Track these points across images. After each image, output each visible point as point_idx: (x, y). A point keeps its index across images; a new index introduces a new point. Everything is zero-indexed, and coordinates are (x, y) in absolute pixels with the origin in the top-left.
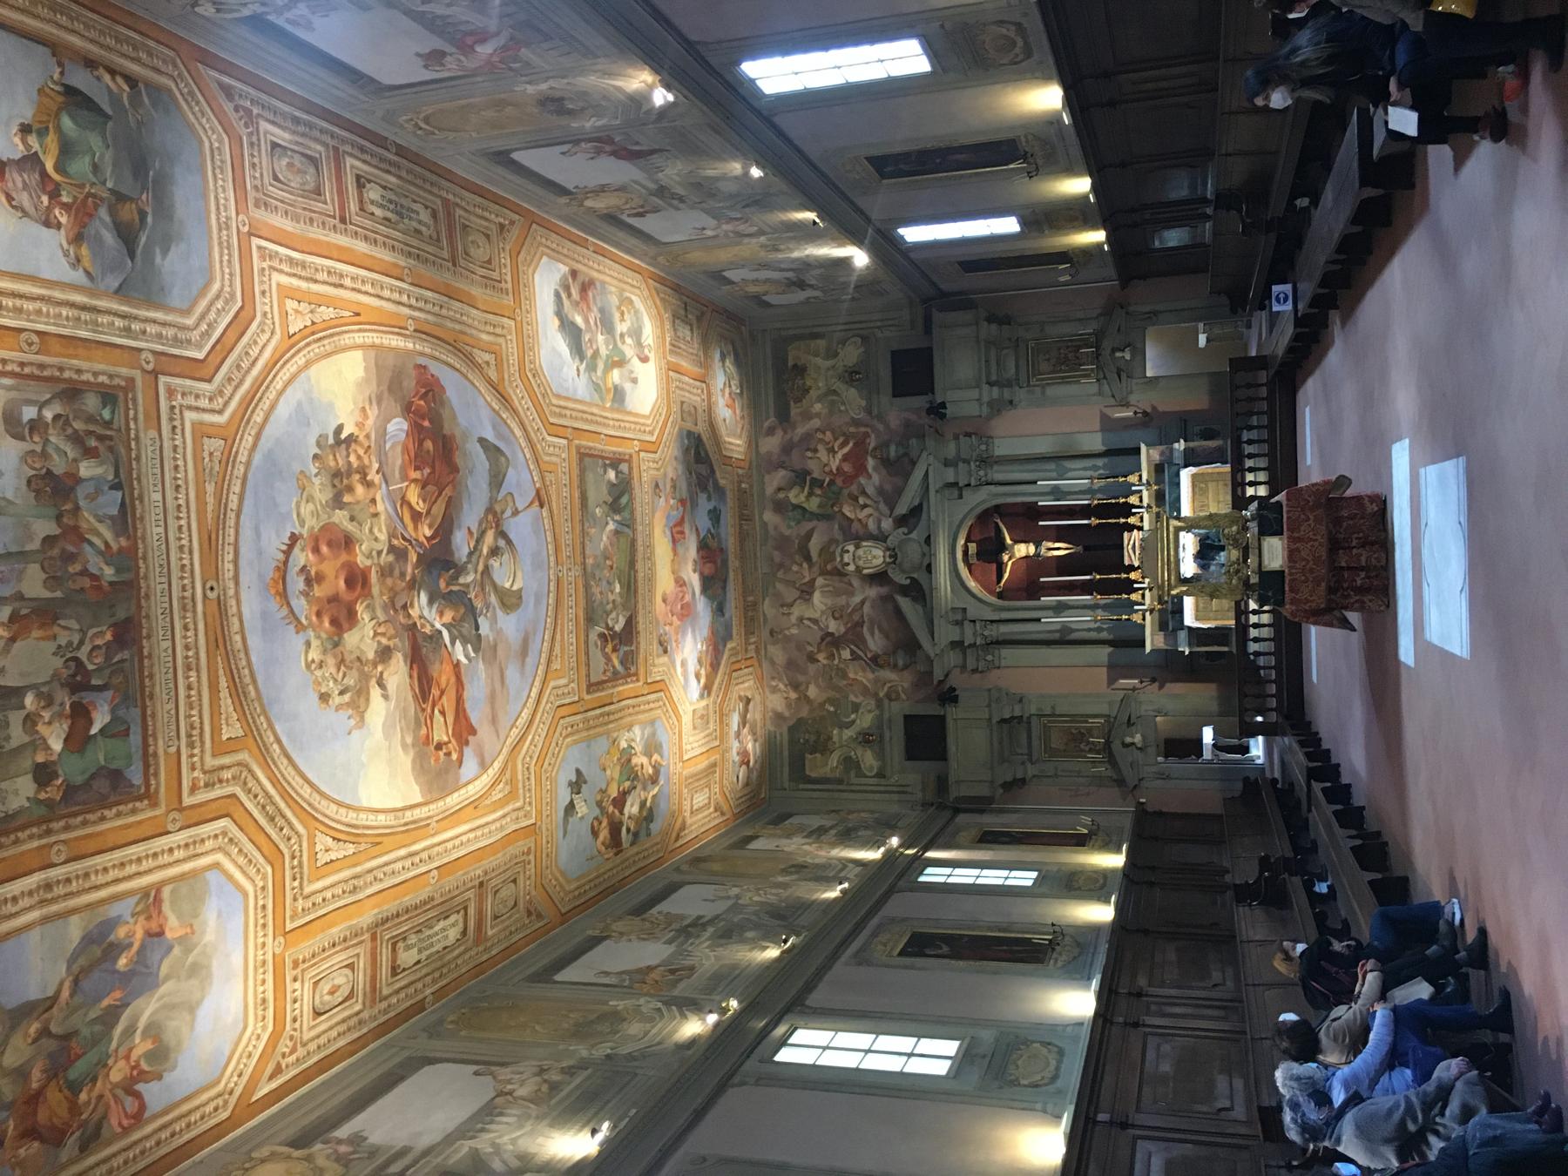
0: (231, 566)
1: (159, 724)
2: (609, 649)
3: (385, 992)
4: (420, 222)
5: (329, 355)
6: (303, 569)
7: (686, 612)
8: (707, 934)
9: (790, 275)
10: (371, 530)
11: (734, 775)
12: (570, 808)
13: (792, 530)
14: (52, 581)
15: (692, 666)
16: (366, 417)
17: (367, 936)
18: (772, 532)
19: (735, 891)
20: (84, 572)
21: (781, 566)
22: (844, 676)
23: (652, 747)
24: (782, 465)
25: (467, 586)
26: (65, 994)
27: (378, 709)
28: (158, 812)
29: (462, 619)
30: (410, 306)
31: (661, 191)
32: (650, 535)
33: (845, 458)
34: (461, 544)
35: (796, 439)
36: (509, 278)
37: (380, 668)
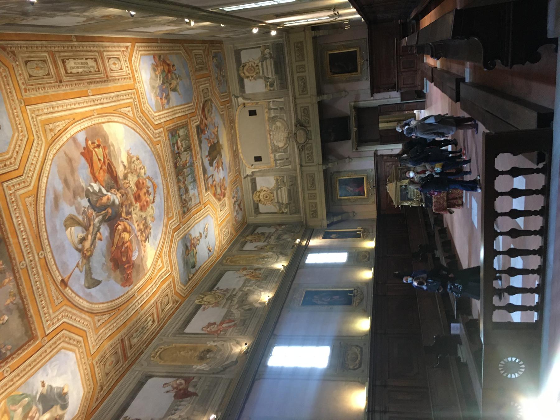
25: (97, 216)
27: (124, 158)
29: (97, 201)
34: (105, 231)
37: (126, 172)
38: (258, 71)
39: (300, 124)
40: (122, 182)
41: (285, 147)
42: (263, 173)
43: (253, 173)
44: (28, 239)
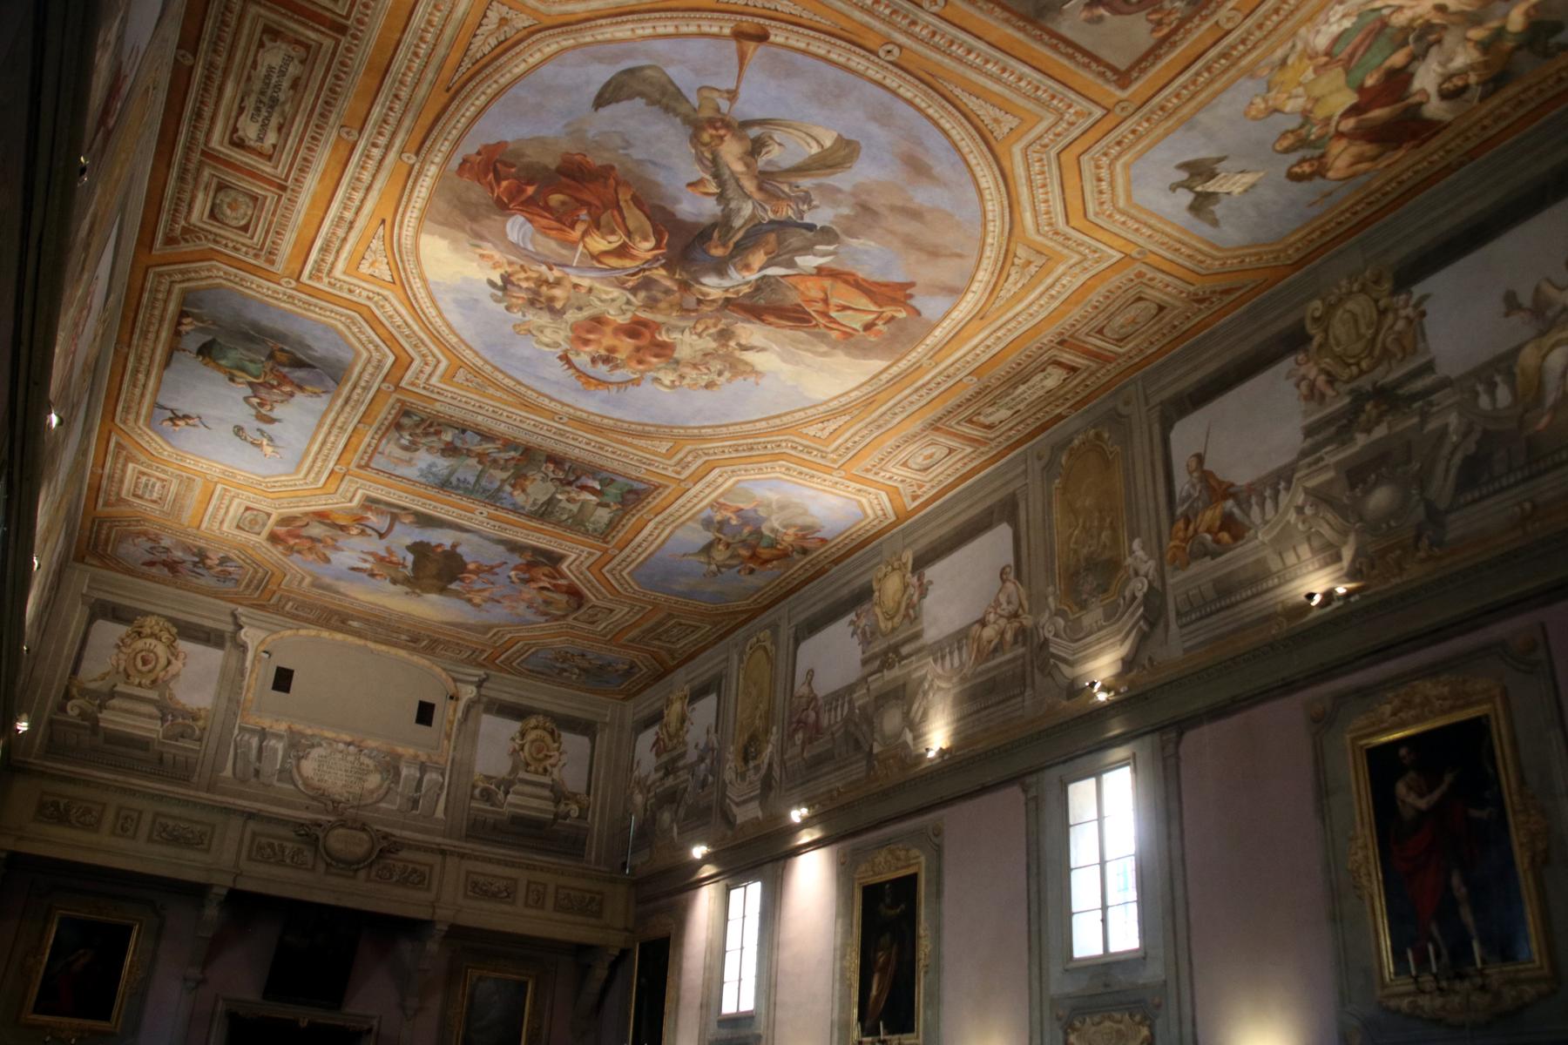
6: (594, 361)
16: (490, 257)
25: (753, 216)
30: (388, 148)
34: (697, 207)
38: (532, 768)
39: (386, 847)
41: (297, 777)
42: (232, 680)
43: (243, 648)
44: (959, 60)
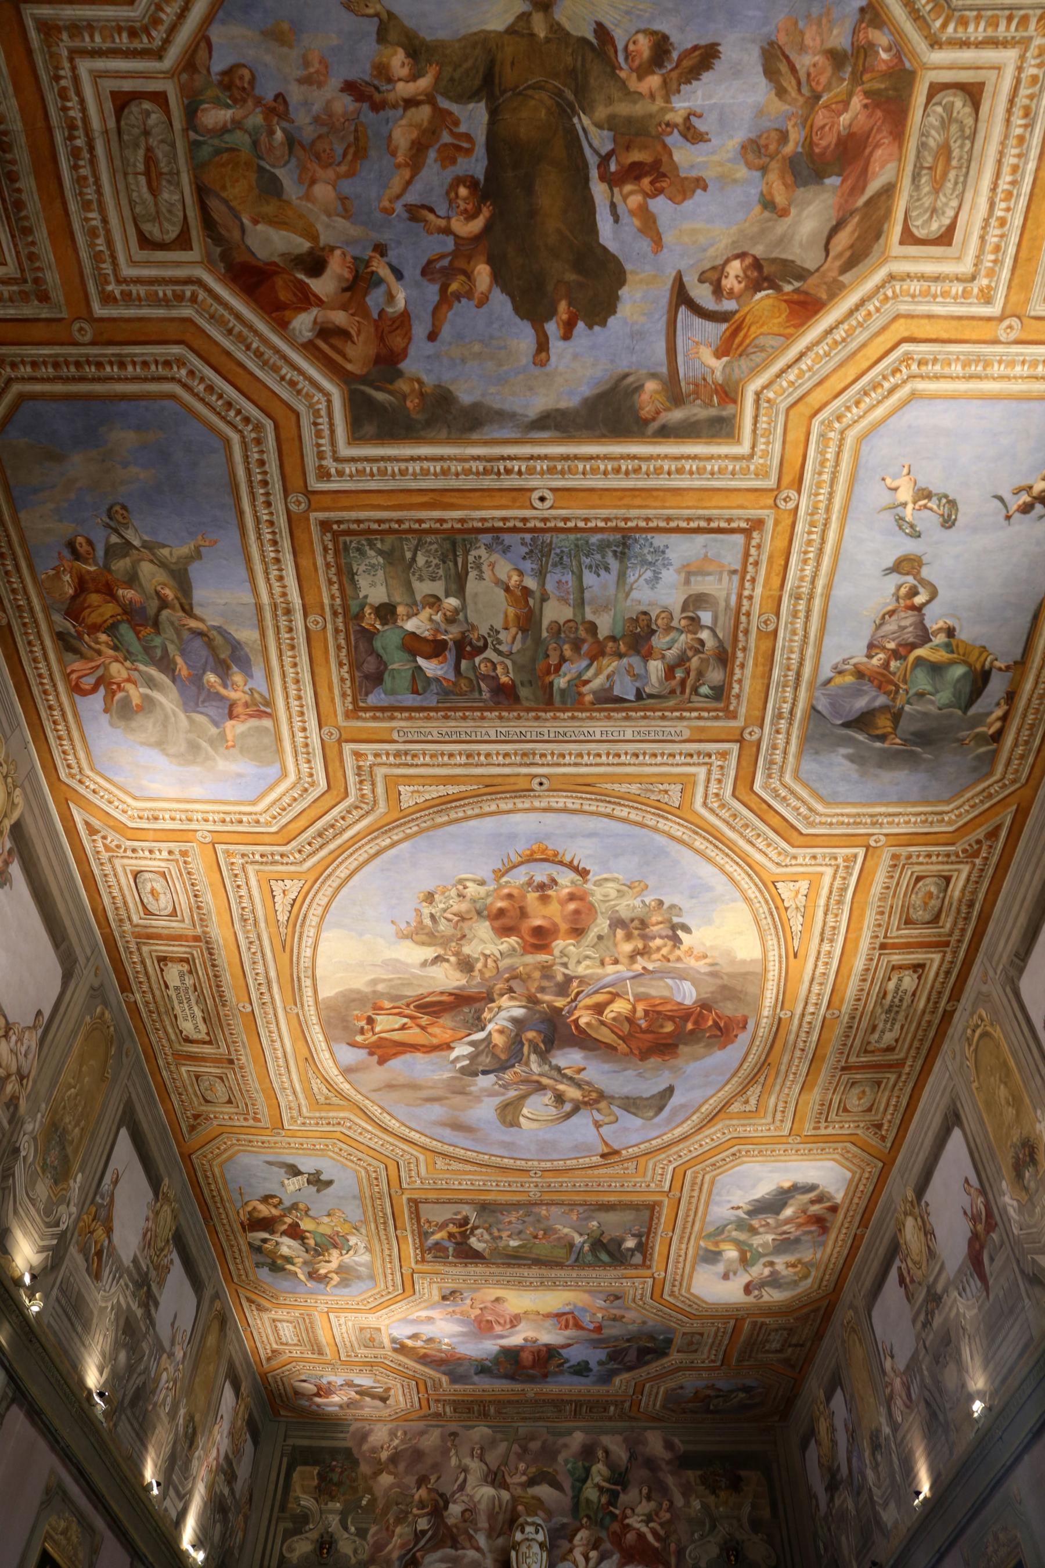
0: (561, 805)
1: (420, 723)
2: (452, 1228)
3: (145, 949)
4: (883, 1032)
5: (757, 923)
6: (554, 882)
7: (483, 1327)
8: (134, 1306)
9: (844, 1471)
10: (587, 957)
11: (307, 1373)
12: (294, 1171)
13: (564, 1463)
14: (557, 629)
15: (427, 1330)
16: (698, 958)
17: (199, 931)
18: (561, 1441)
19: (179, 1354)
20: (563, 659)
21: (525, 1450)
22: (399, 1521)
23: (347, 1275)
24: (633, 1456)
25: (527, 1064)
26: (193, 624)
28: (340, 717)
30: (803, 1015)
31: (934, 1299)
32: (566, 1286)
33: (641, 1536)
34: (569, 1059)
35: (661, 1475)
36: (830, 1131)
37: (453, 959)
40: (473, 983)
